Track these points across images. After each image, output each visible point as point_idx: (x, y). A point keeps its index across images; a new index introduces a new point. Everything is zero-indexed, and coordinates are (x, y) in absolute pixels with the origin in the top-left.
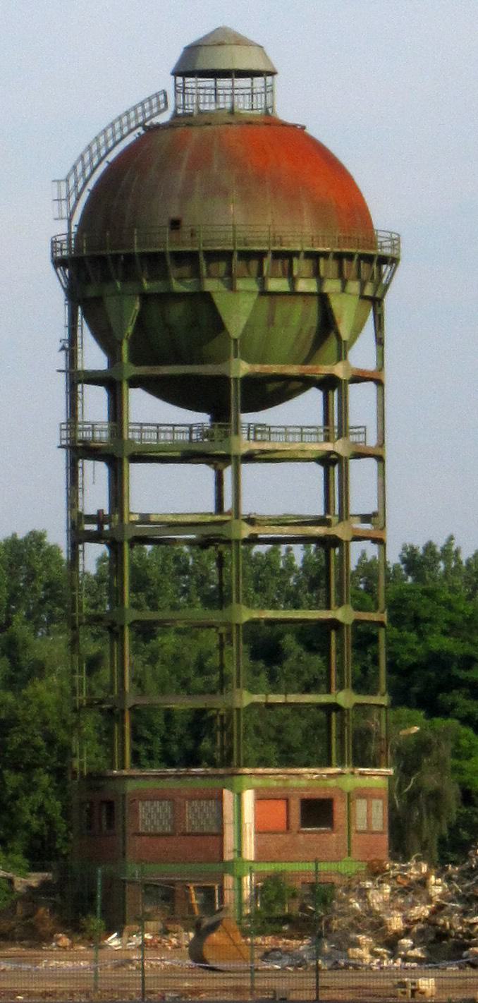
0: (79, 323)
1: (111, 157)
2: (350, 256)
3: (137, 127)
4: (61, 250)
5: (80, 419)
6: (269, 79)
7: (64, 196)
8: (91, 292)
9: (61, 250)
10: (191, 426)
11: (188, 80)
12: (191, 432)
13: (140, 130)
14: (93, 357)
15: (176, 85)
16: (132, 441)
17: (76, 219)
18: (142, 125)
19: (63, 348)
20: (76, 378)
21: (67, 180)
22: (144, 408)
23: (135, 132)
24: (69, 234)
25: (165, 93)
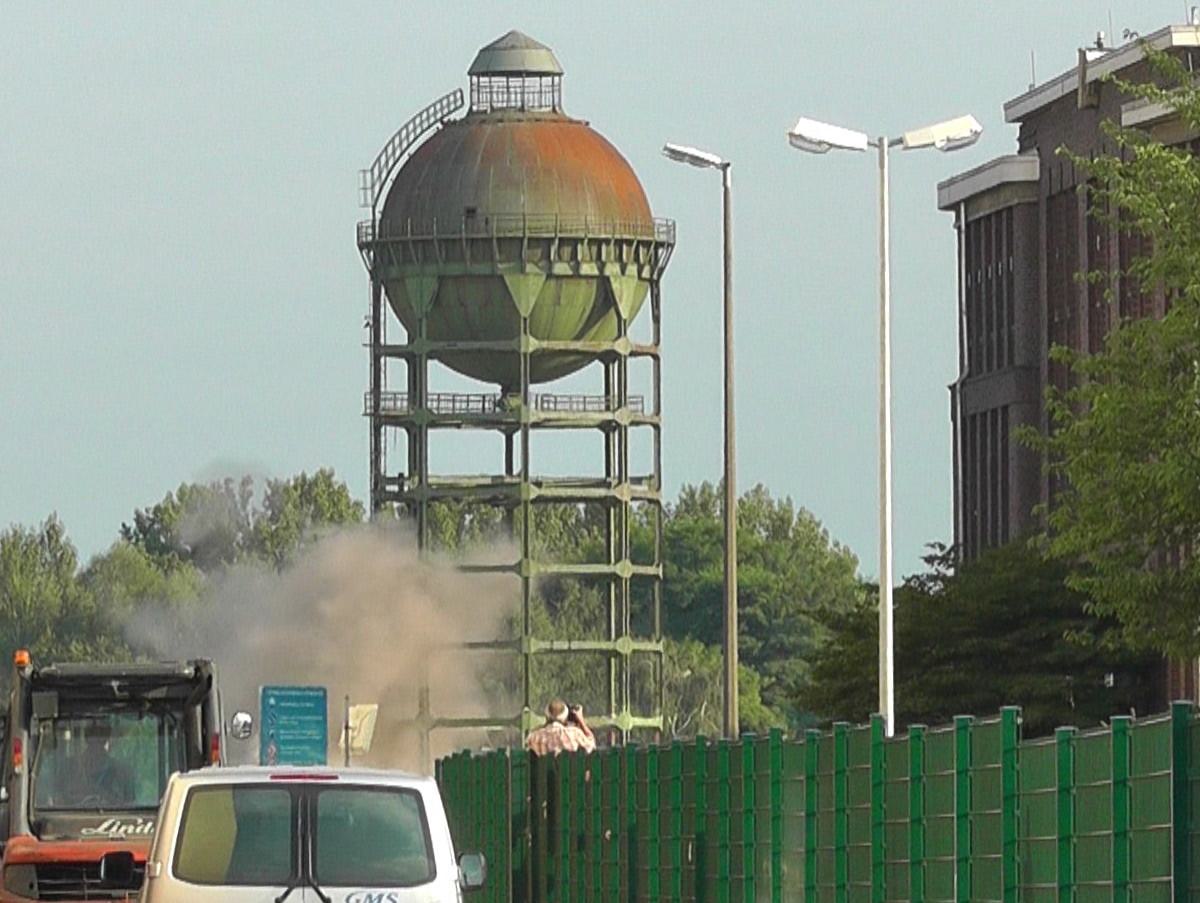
0: (382, 302)
1: (412, 149)
2: (629, 243)
3: (435, 122)
4: (367, 234)
5: (382, 389)
6: (557, 79)
7: (369, 185)
8: (394, 272)
9: (367, 234)
10: (484, 397)
11: (482, 79)
12: (484, 401)
13: (439, 125)
14: (395, 333)
15: (472, 84)
16: (430, 411)
17: (380, 207)
18: (441, 120)
19: (368, 324)
20: (379, 351)
21: (372, 170)
22: (442, 379)
23: (434, 127)
24: (374, 221)
25: (461, 91)
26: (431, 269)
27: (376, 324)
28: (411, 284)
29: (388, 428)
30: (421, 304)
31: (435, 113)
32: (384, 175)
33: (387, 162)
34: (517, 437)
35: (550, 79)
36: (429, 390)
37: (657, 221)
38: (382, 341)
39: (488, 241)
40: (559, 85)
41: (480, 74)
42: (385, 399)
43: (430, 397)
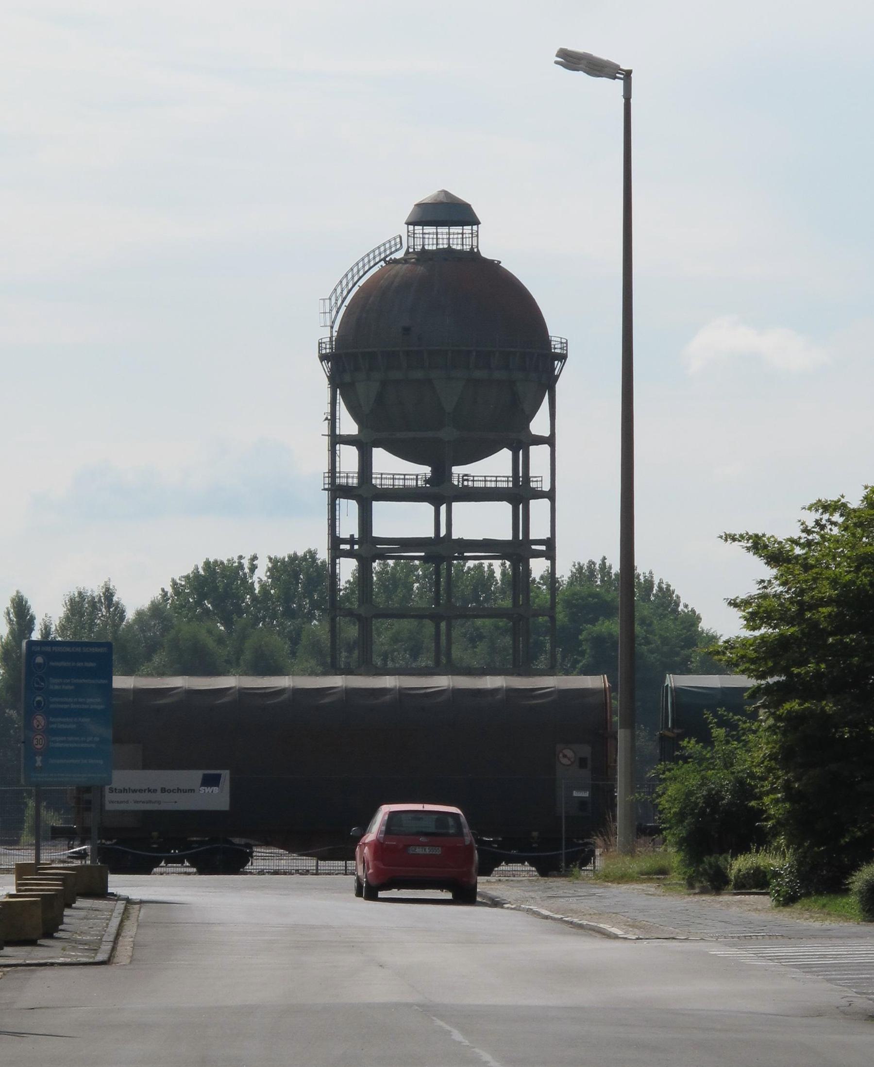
3: (380, 261)
5: (338, 470)
6: (475, 227)
8: (347, 378)
11: (416, 227)
13: (382, 263)
14: (348, 426)
16: (375, 486)
17: (336, 327)
18: (384, 259)
19: (326, 419)
20: (336, 440)
21: (330, 299)
24: (331, 338)
25: (401, 237)
27: (333, 420)
31: (380, 254)
32: (339, 302)
34: (443, 508)
38: (338, 433)
41: (414, 224)
42: (340, 477)
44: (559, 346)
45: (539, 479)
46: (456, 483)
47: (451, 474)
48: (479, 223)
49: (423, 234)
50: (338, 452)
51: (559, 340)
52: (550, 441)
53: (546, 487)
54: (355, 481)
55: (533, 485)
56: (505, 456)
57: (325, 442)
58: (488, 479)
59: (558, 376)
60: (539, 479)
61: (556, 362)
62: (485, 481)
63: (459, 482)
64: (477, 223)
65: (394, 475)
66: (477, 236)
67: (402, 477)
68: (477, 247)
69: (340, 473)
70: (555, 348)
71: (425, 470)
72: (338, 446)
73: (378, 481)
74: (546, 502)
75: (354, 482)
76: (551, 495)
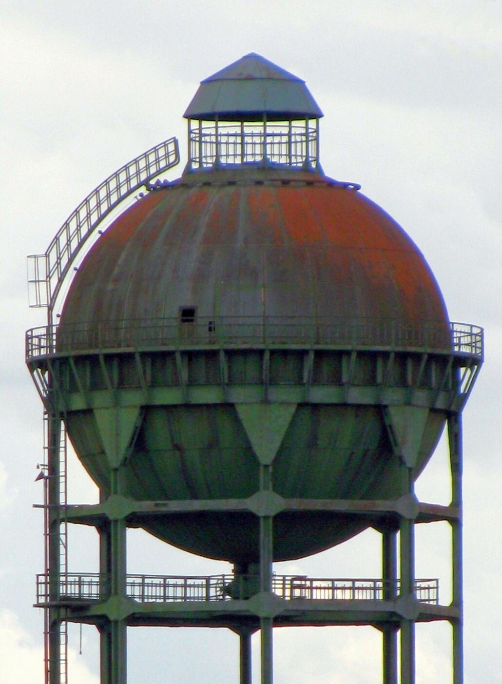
0: (62, 444)
1: (104, 226)
2: (417, 357)
3: (139, 186)
5: (62, 570)
6: (312, 123)
7: (43, 277)
8: (78, 403)
10: (208, 579)
11: (205, 124)
12: (208, 586)
13: (143, 190)
14: (81, 488)
15: (190, 132)
16: (131, 599)
18: (146, 183)
19: (41, 476)
20: (58, 515)
21: (47, 255)
22: (150, 556)
23: (137, 193)
24: (49, 327)
25: (176, 142)
26: (134, 399)
27: (52, 477)
28: (103, 419)
29: (69, 623)
30: (116, 444)
31: (138, 173)
32: (64, 261)
33: (68, 244)
34: (256, 638)
35: (302, 123)
36: (130, 569)
37: (456, 327)
38: (62, 501)
39: (211, 355)
40: (317, 131)
41: (201, 117)
42: (66, 583)
43: (129, 580)
44: (466, 340)
45: (432, 584)
46: (279, 592)
47: (269, 576)
48: (321, 116)
49: (266, 135)
50: (62, 537)
51: (467, 329)
52: (452, 515)
53: (446, 600)
54: (95, 590)
55: (420, 595)
56: (370, 540)
57: (39, 518)
58: (339, 584)
59: (466, 396)
60: (432, 584)
61: (462, 370)
62: (334, 588)
63: (284, 589)
64: (316, 115)
65: (165, 578)
66: (317, 139)
67: (181, 582)
68: (317, 159)
69: (66, 575)
70: (459, 345)
71: (224, 569)
72: (62, 526)
73: (137, 591)
74: (444, 627)
75: (92, 591)
76: (453, 616)
